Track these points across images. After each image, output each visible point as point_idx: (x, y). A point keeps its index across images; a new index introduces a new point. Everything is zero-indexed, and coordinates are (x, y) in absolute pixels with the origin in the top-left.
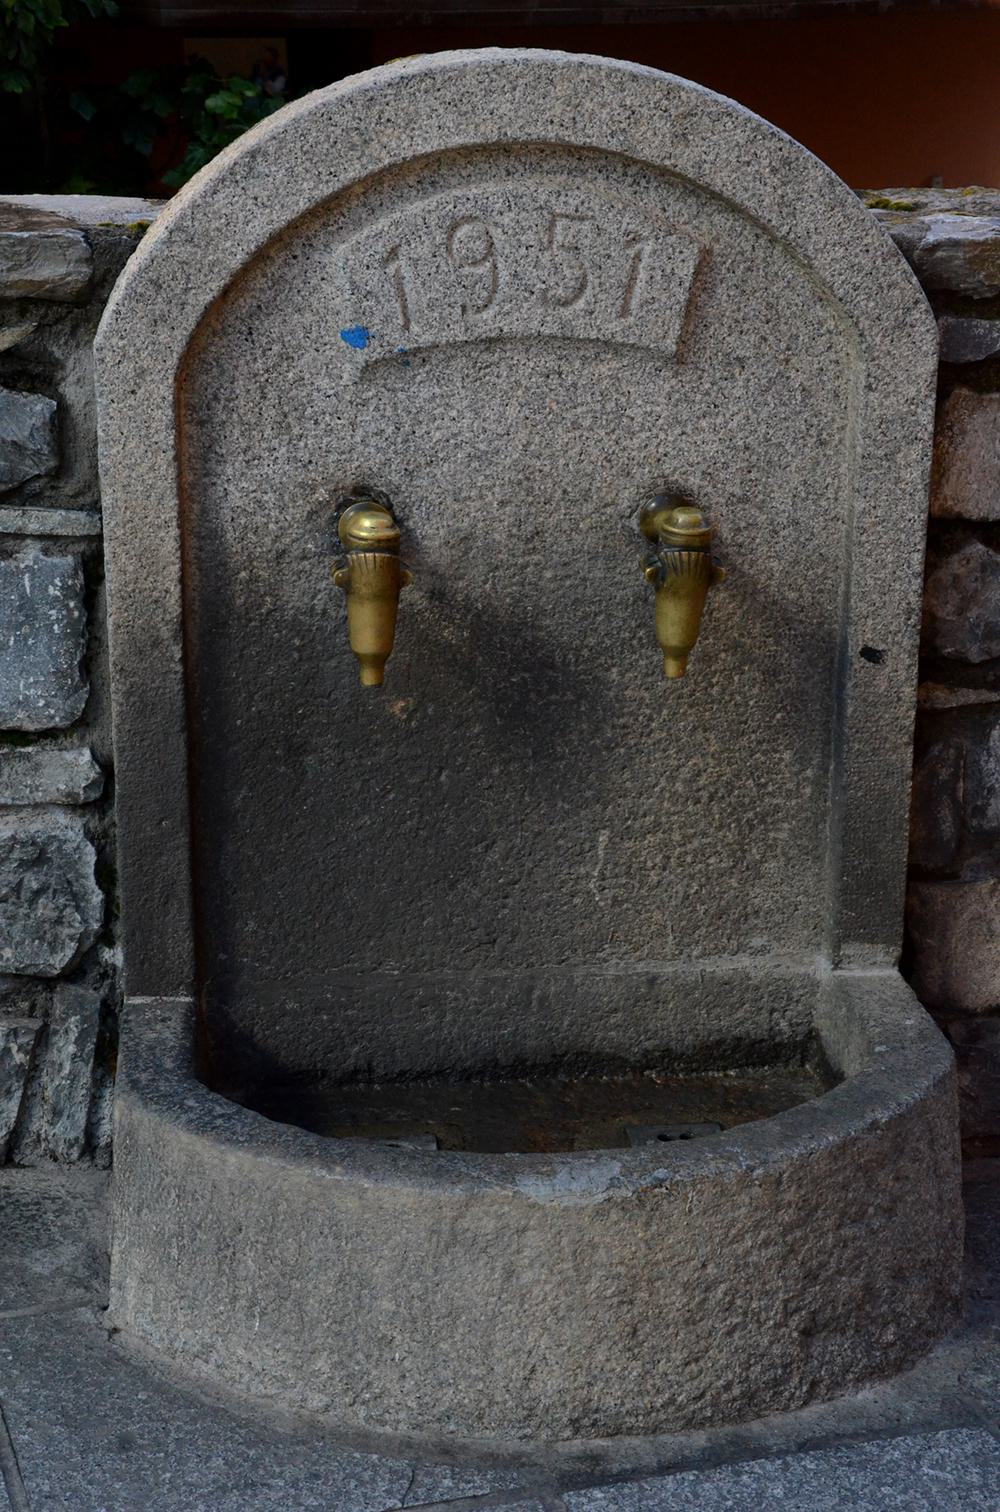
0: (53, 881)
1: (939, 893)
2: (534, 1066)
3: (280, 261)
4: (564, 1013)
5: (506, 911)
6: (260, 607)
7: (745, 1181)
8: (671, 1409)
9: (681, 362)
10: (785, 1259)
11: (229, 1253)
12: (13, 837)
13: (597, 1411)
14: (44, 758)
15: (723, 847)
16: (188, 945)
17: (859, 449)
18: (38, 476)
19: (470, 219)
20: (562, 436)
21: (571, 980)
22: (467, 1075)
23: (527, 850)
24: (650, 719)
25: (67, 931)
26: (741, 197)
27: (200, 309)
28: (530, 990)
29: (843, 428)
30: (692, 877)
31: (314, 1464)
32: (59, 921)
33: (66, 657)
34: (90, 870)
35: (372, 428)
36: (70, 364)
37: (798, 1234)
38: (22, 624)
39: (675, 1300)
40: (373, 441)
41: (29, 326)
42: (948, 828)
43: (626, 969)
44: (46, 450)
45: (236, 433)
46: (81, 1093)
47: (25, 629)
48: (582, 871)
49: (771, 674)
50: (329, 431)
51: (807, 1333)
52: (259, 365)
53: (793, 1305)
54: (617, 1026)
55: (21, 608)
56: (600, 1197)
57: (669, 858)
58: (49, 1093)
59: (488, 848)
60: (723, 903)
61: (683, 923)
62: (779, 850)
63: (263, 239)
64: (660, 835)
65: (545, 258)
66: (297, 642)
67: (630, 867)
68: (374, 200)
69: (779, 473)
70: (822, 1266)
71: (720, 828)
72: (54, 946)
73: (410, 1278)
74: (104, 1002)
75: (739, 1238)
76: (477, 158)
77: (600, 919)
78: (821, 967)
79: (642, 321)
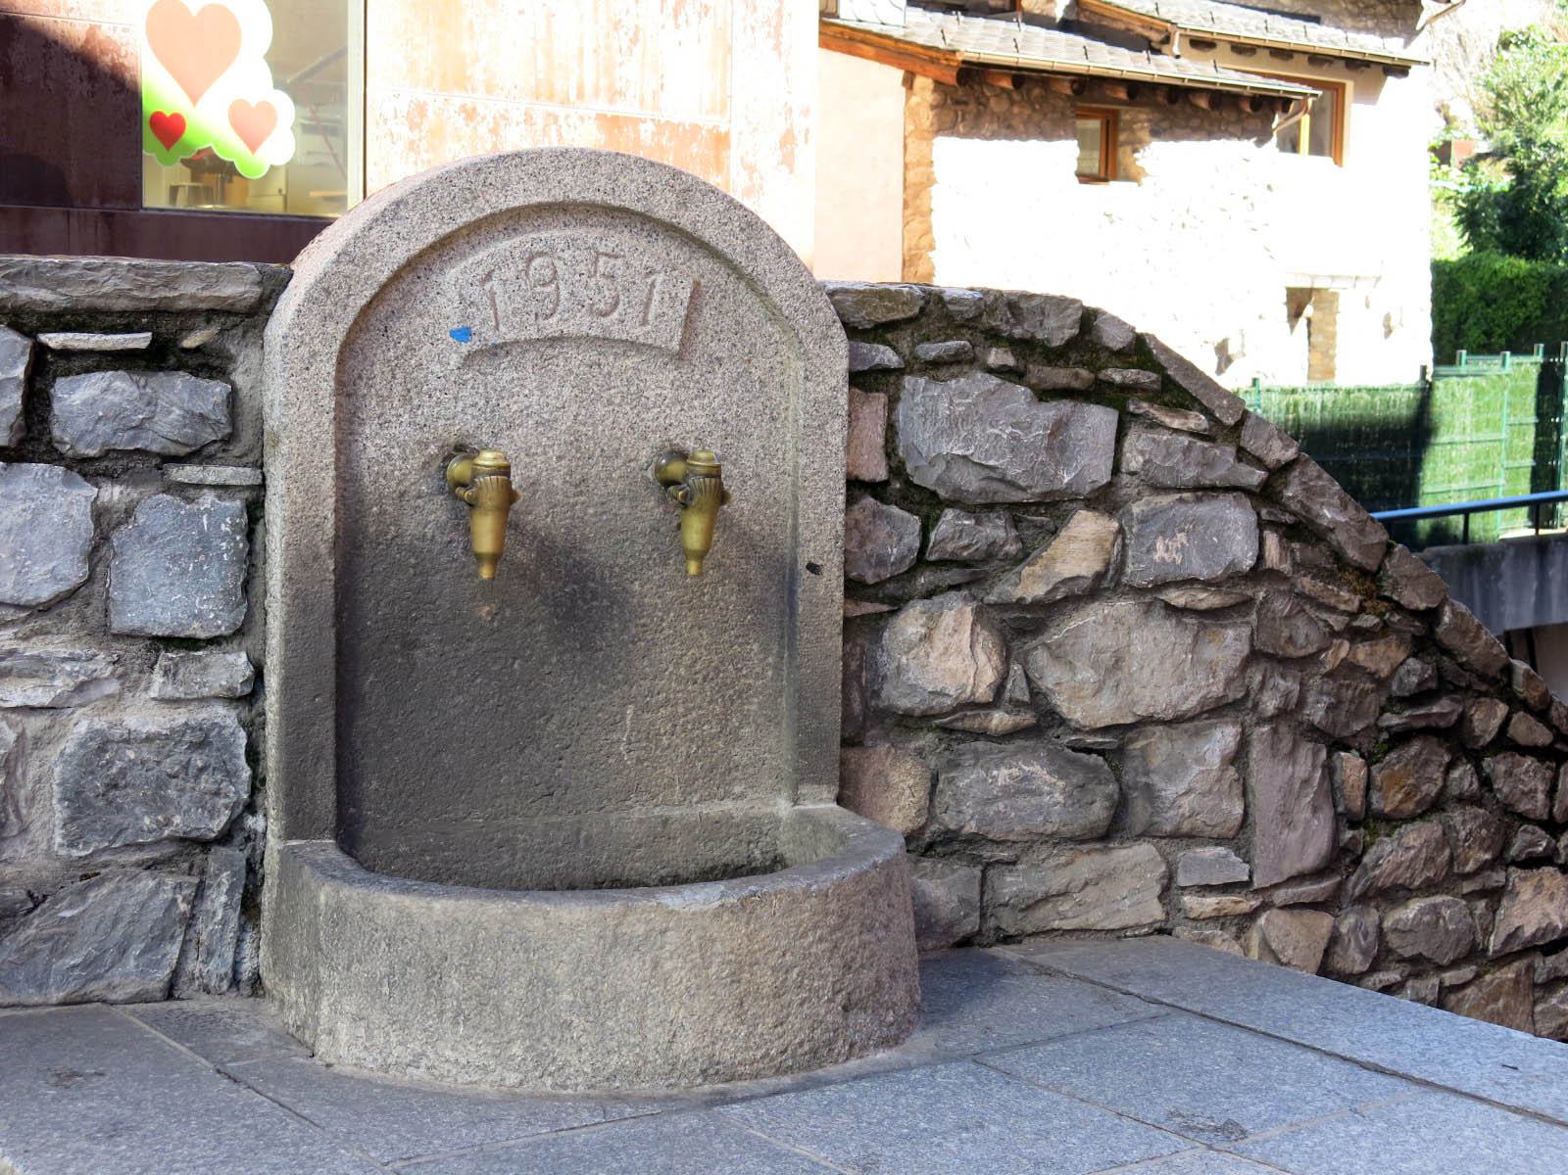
0: (212, 761)
1: (853, 754)
3: (408, 280)
4: (603, 849)
6: (387, 534)
7: (807, 894)
8: (767, 1060)
9: (681, 359)
10: (832, 952)
11: (436, 979)
12: (186, 724)
13: (718, 1063)
14: (212, 659)
16: (333, 797)
17: (801, 422)
18: (215, 442)
19: (541, 254)
20: (600, 410)
24: (662, 620)
25: (223, 801)
26: (721, 246)
27: (357, 310)
28: (578, 833)
29: (787, 409)
30: (692, 740)
32: (217, 793)
33: (233, 578)
34: (242, 751)
35: (469, 402)
36: (241, 359)
37: (839, 935)
38: (199, 554)
39: (767, 980)
40: (470, 411)
41: (214, 329)
42: (857, 707)
44: (224, 420)
45: (374, 403)
46: (230, 935)
47: (202, 558)
48: (615, 737)
49: (744, 586)
50: (439, 403)
51: (845, 1009)
52: (391, 354)
53: (838, 986)
54: (641, 858)
55: (199, 541)
56: (717, 904)
58: (203, 937)
59: (548, 720)
63: (403, 262)
65: (592, 283)
66: (413, 561)
68: (474, 239)
69: (746, 439)
70: (853, 959)
71: (710, 703)
72: (213, 814)
73: (584, 975)
74: (248, 860)
75: (804, 935)
76: (544, 214)
78: (783, 807)
79: (656, 328)
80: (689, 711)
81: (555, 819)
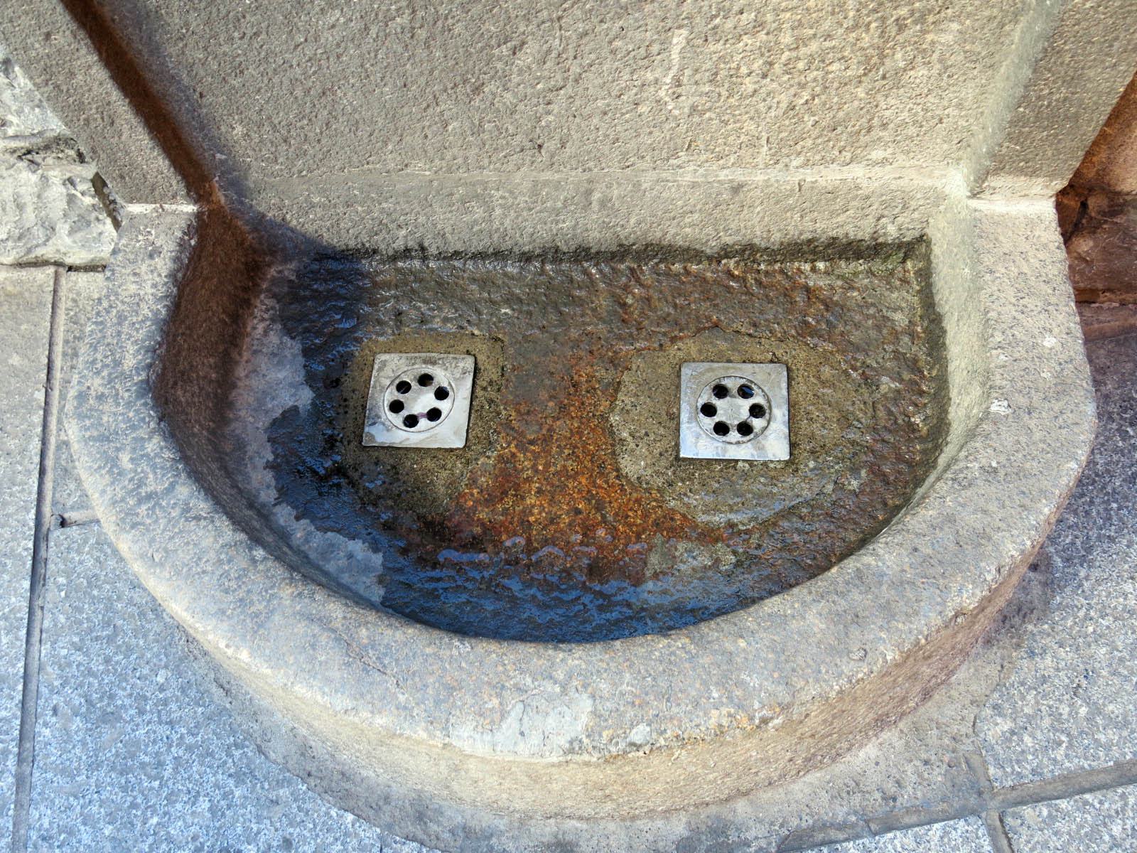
2: (598, 253)
5: (551, 118)
15: (852, 51)
21: (637, 185)
22: (527, 258)
23: (571, 53)
28: (589, 193)
30: (802, 86)
31: (291, 824)
43: (705, 176)
48: (650, 76)
54: (692, 225)
57: (771, 64)
60: (841, 114)
61: (783, 135)
62: (935, 56)
64: (762, 36)
67: (716, 74)
77: (673, 129)
78: (956, 181)
80: (800, 42)
81: (547, 175)
